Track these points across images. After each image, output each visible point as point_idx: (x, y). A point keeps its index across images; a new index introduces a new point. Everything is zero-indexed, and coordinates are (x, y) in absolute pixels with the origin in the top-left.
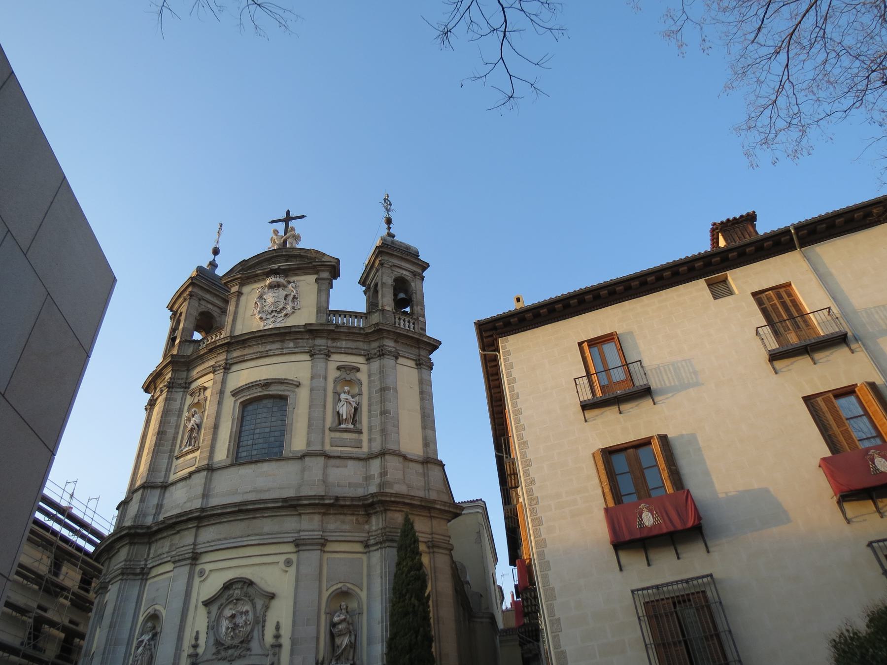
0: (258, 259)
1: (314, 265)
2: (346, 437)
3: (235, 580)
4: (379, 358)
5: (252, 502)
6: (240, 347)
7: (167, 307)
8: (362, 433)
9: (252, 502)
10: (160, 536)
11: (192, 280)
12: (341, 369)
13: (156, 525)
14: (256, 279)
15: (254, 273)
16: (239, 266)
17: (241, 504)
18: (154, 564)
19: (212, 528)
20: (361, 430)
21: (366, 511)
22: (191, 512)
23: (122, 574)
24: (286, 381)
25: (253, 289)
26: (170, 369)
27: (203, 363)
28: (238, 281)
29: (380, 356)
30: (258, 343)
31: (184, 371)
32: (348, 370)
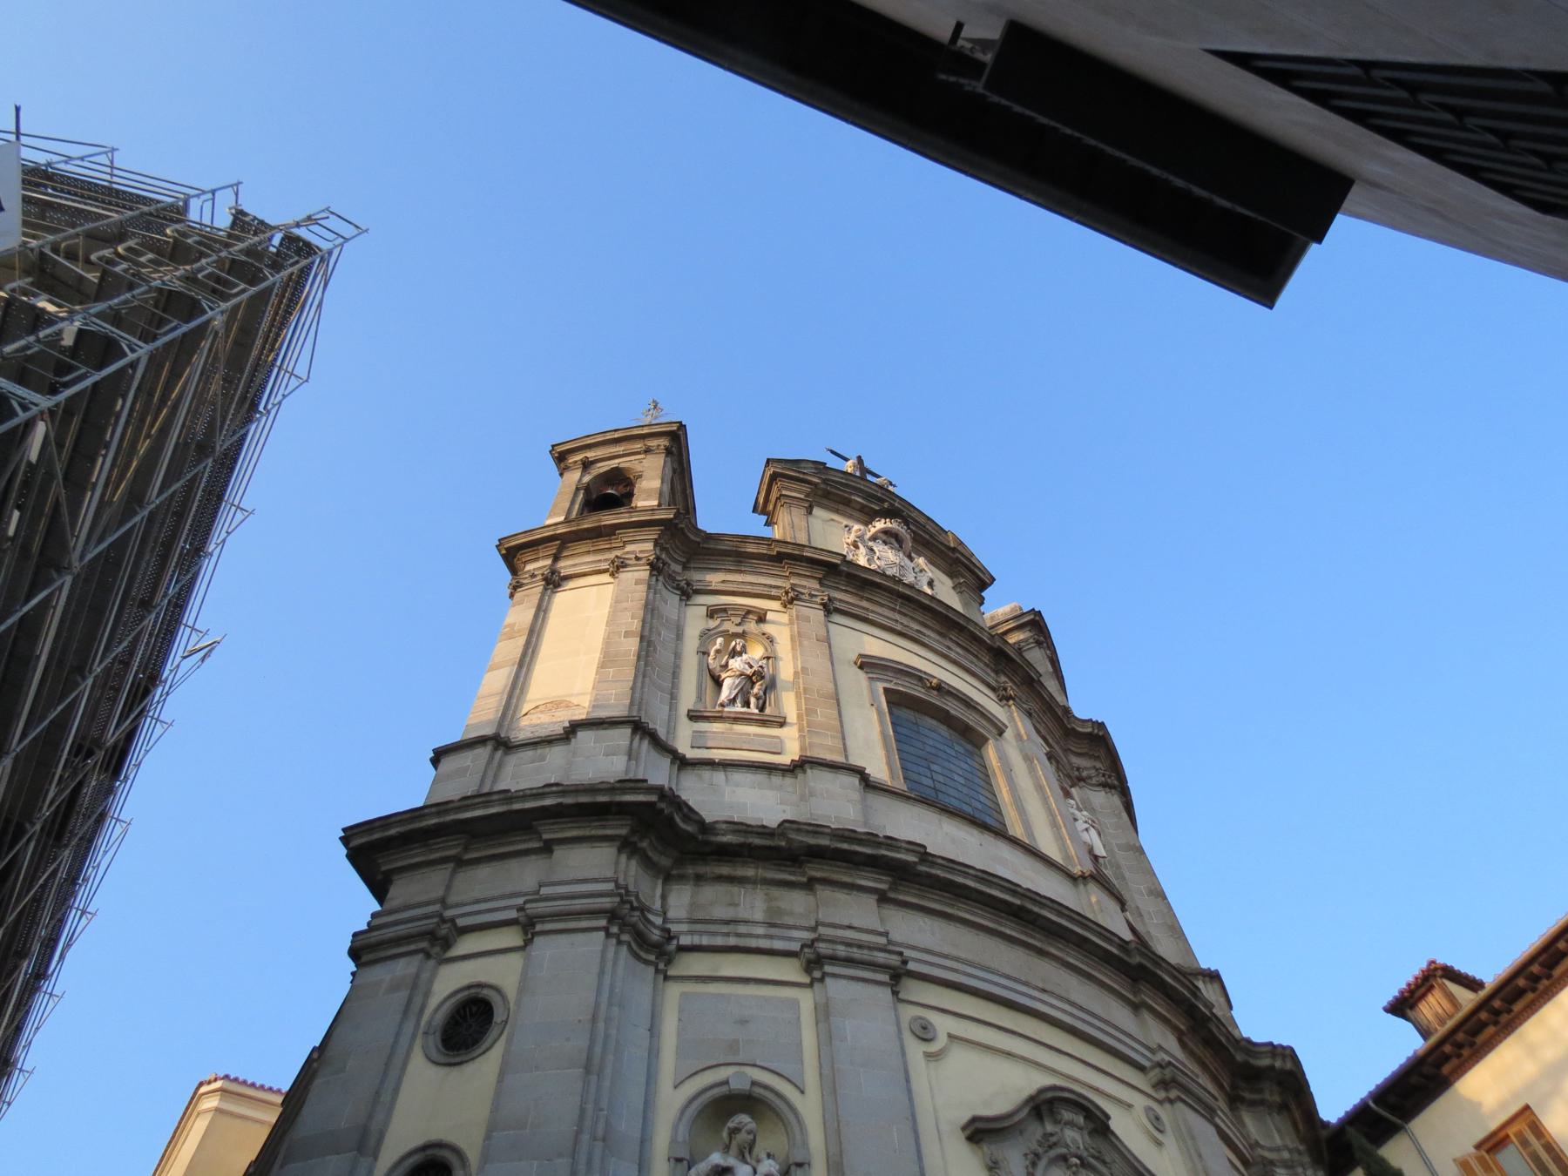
0: (846, 480)
1: (957, 558)
3: (1067, 1095)
5: (1056, 906)
6: (848, 589)
7: (553, 446)
9: (1056, 906)
10: (725, 870)
11: (679, 429)
13: (735, 832)
14: (841, 507)
15: (846, 495)
16: (811, 465)
17: (1028, 894)
18: (696, 940)
19: (924, 922)
21: (1234, 1087)
22: (891, 842)
23: (613, 915)
24: (979, 708)
25: (833, 520)
26: (653, 533)
27: (741, 572)
28: (806, 488)
30: (893, 606)
31: (676, 561)
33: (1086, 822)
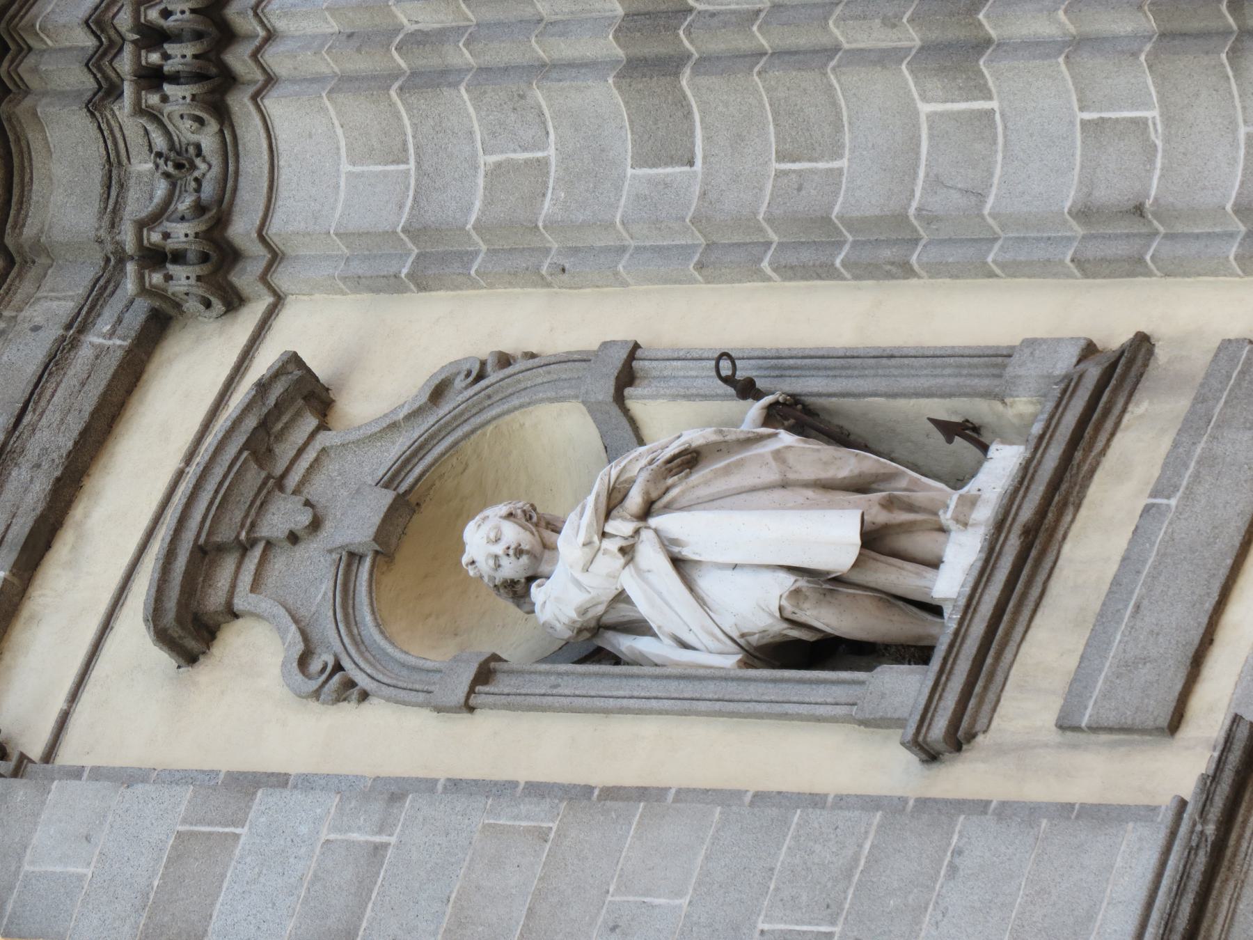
2: (1119, 542)
4: (239, 102)
8: (1142, 344)
12: (215, 599)
20: (1089, 350)
29: (229, 80)
32: (261, 504)
33: (627, 552)
